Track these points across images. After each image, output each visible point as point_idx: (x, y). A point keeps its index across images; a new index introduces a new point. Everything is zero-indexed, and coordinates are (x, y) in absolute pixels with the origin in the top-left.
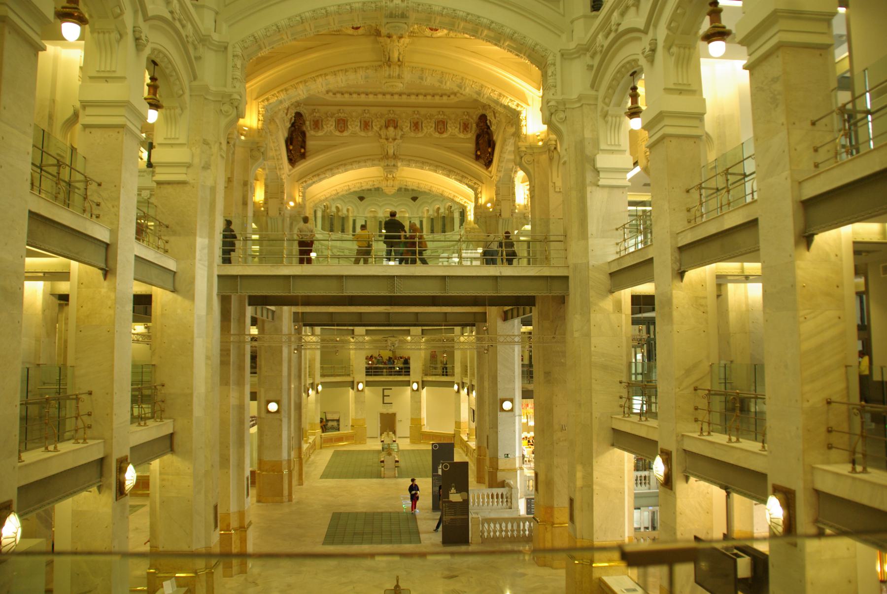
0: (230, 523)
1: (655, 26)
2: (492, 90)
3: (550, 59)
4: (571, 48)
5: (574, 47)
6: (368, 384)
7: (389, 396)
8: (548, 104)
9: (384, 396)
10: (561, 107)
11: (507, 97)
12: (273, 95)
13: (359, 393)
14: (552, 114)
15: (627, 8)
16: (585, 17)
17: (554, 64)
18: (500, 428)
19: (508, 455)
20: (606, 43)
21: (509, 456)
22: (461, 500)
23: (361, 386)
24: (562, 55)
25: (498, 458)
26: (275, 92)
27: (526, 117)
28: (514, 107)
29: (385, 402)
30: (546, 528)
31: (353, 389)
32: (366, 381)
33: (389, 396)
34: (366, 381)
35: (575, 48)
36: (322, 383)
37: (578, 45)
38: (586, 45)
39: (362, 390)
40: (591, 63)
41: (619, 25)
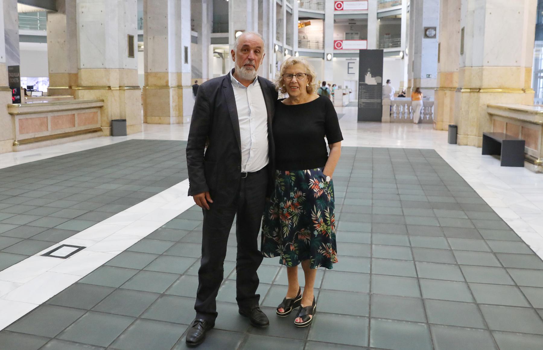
0: (168, 80)
6: (335, 55)
7: (352, 68)
9: (349, 68)
13: (328, 62)
18: (423, 52)
19: (429, 75)
21: (430, 76)
22: (376, 84)
23: (329, 57)
25: (420, 78)
29: (349, 72)
30: (445, 94)
31: (324, 58)
32: (334, 54)
33: (352, 68)
34: (334, 54)
36: (299, 52)
39: (331, 60)
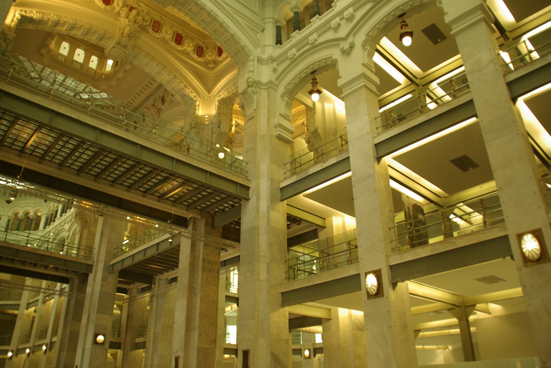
1: (354, 36)
2: (181, 81)
3: (252, 57)
4: (263, 58)
5: (266, 57)
8: (248, 80)
10: (255, 85)
11: (189, 89)
12: (31, 12)
14: (249, 86)
15: (330, 28)
16: (273, 46)
17: (254, 61)
20: (297, 54)
24: (258, 60)
26: (34, 11)
27: (199, 105)
28: (192, 96)
35: (267, 58)
37: (271, 56)
38: (274, 58)
40: (276, 67)
41: (316, 40)
